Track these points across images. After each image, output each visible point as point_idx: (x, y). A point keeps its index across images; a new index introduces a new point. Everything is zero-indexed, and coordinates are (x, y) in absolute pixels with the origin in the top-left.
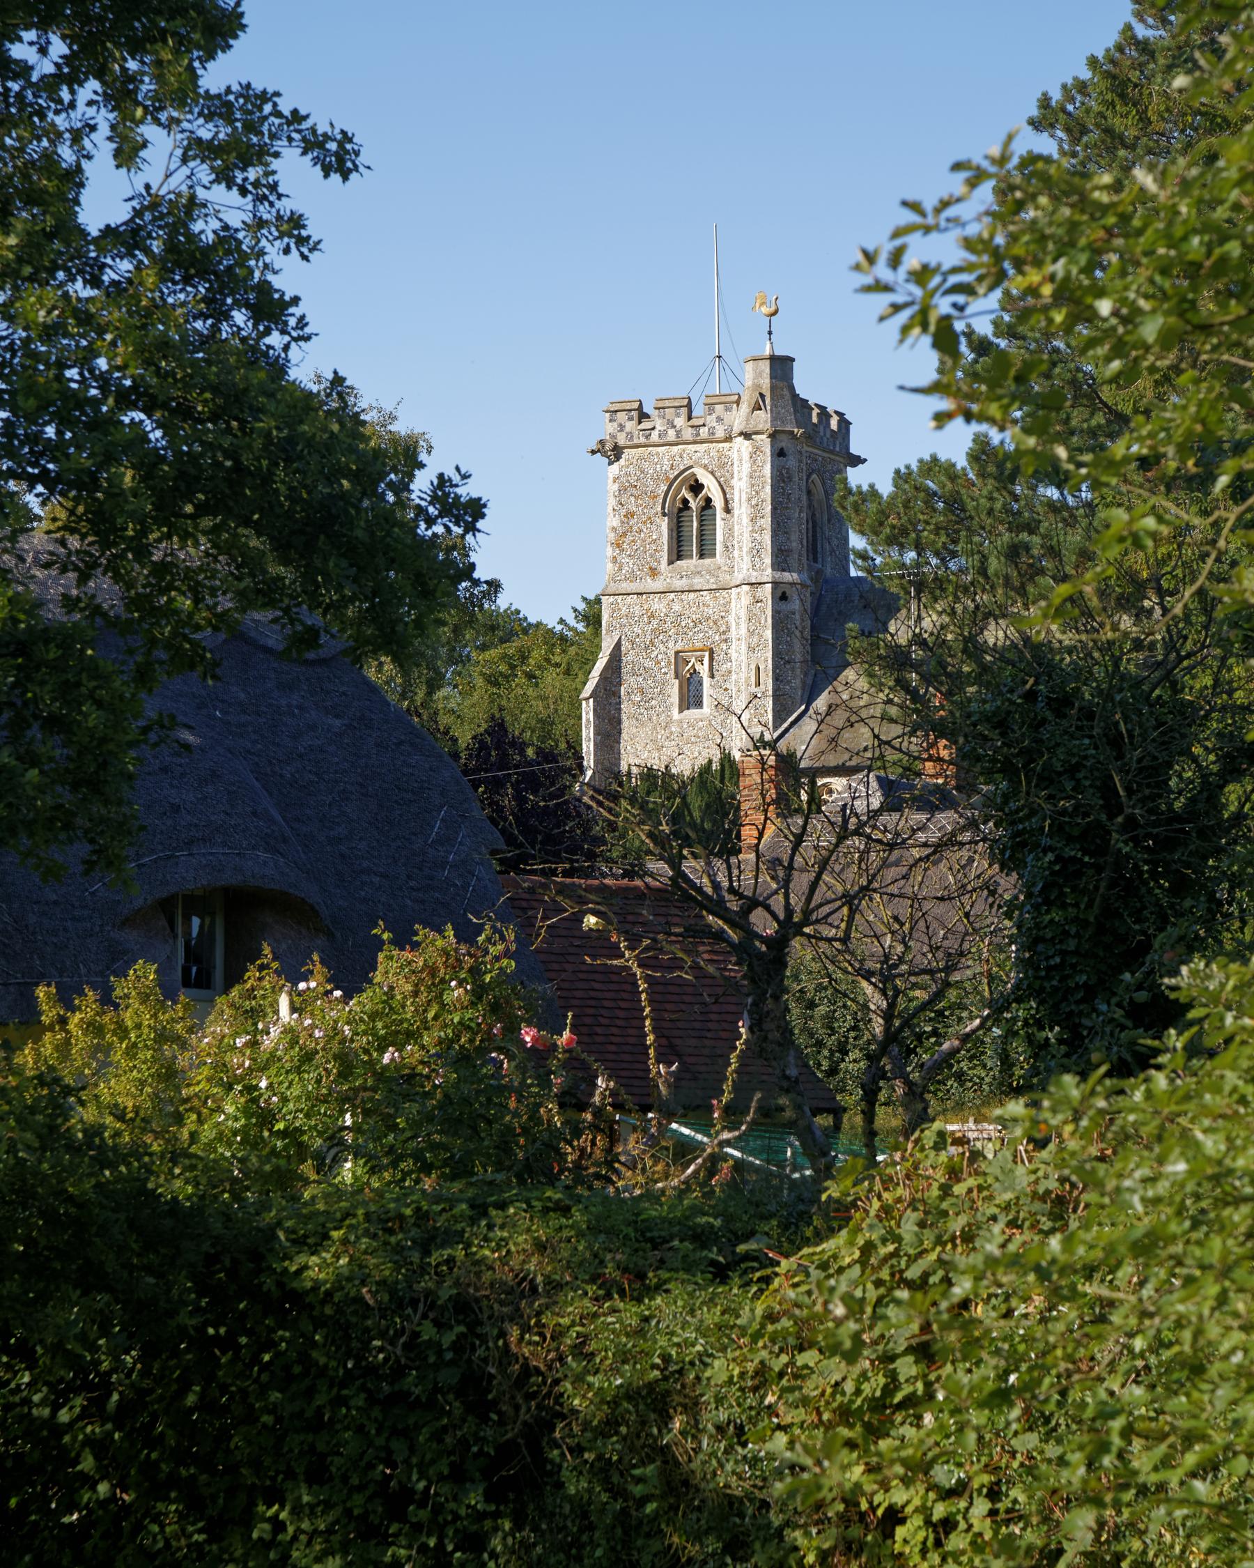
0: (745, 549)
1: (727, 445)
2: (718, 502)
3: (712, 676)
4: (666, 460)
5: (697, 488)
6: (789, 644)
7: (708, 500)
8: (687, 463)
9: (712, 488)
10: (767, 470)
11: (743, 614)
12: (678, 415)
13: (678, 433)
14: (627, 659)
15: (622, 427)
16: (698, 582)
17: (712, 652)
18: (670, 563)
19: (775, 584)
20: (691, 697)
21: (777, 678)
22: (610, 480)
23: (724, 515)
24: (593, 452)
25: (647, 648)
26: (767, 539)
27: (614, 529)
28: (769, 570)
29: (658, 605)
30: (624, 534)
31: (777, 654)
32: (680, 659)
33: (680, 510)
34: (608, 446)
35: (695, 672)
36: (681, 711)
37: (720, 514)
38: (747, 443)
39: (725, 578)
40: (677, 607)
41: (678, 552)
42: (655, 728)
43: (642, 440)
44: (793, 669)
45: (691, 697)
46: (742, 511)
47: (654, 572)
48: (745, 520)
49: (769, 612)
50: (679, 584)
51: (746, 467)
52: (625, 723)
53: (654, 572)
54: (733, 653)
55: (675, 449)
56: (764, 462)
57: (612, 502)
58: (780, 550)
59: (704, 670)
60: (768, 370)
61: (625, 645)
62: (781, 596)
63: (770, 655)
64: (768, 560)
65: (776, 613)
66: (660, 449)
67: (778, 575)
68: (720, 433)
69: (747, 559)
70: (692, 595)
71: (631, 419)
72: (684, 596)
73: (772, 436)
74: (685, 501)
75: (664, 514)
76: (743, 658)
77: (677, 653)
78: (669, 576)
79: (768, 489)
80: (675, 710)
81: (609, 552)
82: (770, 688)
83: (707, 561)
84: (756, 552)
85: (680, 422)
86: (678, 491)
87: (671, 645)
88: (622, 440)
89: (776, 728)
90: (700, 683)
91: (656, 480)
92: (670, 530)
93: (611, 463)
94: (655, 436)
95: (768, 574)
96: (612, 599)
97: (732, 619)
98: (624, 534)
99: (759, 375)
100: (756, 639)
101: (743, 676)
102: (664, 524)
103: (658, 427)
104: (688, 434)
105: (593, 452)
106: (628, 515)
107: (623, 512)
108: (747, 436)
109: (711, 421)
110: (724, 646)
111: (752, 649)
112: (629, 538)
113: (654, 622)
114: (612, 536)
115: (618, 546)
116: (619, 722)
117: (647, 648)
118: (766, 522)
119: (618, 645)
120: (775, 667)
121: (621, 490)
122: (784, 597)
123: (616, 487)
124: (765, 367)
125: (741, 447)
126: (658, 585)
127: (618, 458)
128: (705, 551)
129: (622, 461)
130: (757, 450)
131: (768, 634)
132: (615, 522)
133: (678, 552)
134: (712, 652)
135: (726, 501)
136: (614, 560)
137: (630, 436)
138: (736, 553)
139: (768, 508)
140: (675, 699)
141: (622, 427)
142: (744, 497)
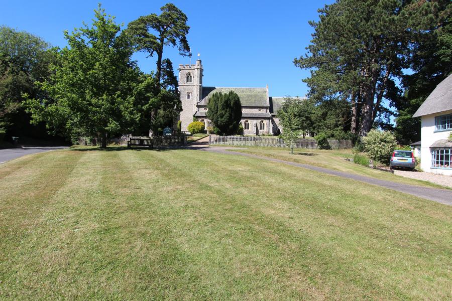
2: (192, 76)
5: (190, 74)
9: (191, 75)
20: (189, 97)
45: (189, 97)
46: (196, 77)
59: (190, 94)
108: (197, 69)
133: (187, 81)
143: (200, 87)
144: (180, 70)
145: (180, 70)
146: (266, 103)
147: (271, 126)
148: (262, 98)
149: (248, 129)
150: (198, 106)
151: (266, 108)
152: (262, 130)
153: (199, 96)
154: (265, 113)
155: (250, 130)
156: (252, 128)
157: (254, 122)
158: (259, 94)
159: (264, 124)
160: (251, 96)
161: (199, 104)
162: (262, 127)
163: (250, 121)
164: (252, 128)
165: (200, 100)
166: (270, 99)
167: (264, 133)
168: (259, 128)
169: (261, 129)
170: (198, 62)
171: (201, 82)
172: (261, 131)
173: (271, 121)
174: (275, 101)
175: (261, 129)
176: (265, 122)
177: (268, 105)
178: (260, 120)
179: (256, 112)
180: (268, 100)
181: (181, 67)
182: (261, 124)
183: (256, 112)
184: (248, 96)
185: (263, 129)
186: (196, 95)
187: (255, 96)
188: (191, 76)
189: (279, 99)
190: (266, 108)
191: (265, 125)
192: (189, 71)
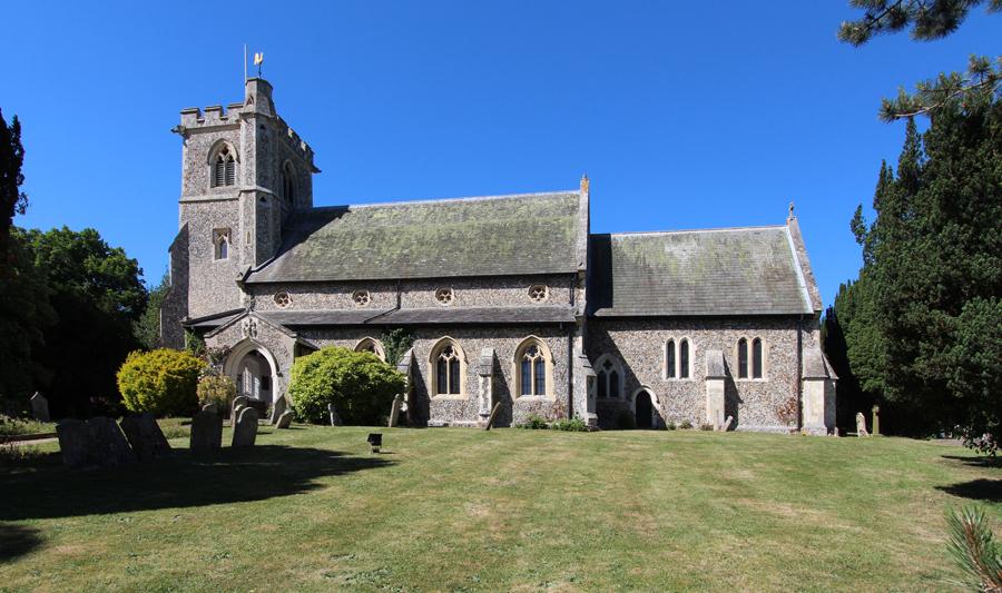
2: (235, 157)
5: (225, 151)
7: (231, 157)
9: (233, 153)
10: (254, 134)
15: (189, 120)
16: (224, 196)
18: (212, 187)
19: (258, 192)
20: (221, 253)
21: (258, 240)
26: (254, 169)
29: (205, 206)
31: (258, 227)
35: (224, 241)
36: (216, 259)
37: (236, 163)
41: (216, 182)
43: (199, 126)
47: (204, 192)
49: (254, 206)
50: (216, 197)
61: (190, 226)
62: (261, 199)
63: (254, 227)
64: (254, 180)
74: (220, 158)
79: (254, 143)
80: (213, 258)
83: (230, 187)
84: (249, 176)
89: (257, 265)
92: (212, 172)
111: (246, 224)
114: (184, 174)
116: (188, 264)
118: (254, 160)
119: (186, 226)
122: (263, 200)
128: (229, 182)
131: (254, 216)
133: (216, 182)
136: (186, 185)
140: (213, 253)
144: (186, 133)
145: (186, 133)
146: (568, 258)
147: (582, 371)
148: (553, 236)
149: (455, 389)
150: (251, 288)
151: (570, 280)
152: (532, 398)
154: (565, 304)
155: (462, 395)
156: (472, 383)
157: (485, 349)
158: (540, 220)
159: (540, 362)
160: (502, 231)
162: (532, 378)
163: (459, 347)
164: (472, 383)
167: (541, 415)
168: (513, 387)
169: (524, 389)
170: (251, 89)
172: (523, 404)
173: (579, 343)
174: (626, 249)
175: (524, 389)
176: (547, 348)
177: (579, 260)
178: (517, 342)
179: (516, 301)
181: (189, 122)
182: (523, 364)
183: (516, 301)
184: (486, 232)
185: (540, 389)
187: (521, 229)
188: (231, 160)
189: (645, 240)
190: (570, 280)
191: (548, 366)
192: (220, 135)
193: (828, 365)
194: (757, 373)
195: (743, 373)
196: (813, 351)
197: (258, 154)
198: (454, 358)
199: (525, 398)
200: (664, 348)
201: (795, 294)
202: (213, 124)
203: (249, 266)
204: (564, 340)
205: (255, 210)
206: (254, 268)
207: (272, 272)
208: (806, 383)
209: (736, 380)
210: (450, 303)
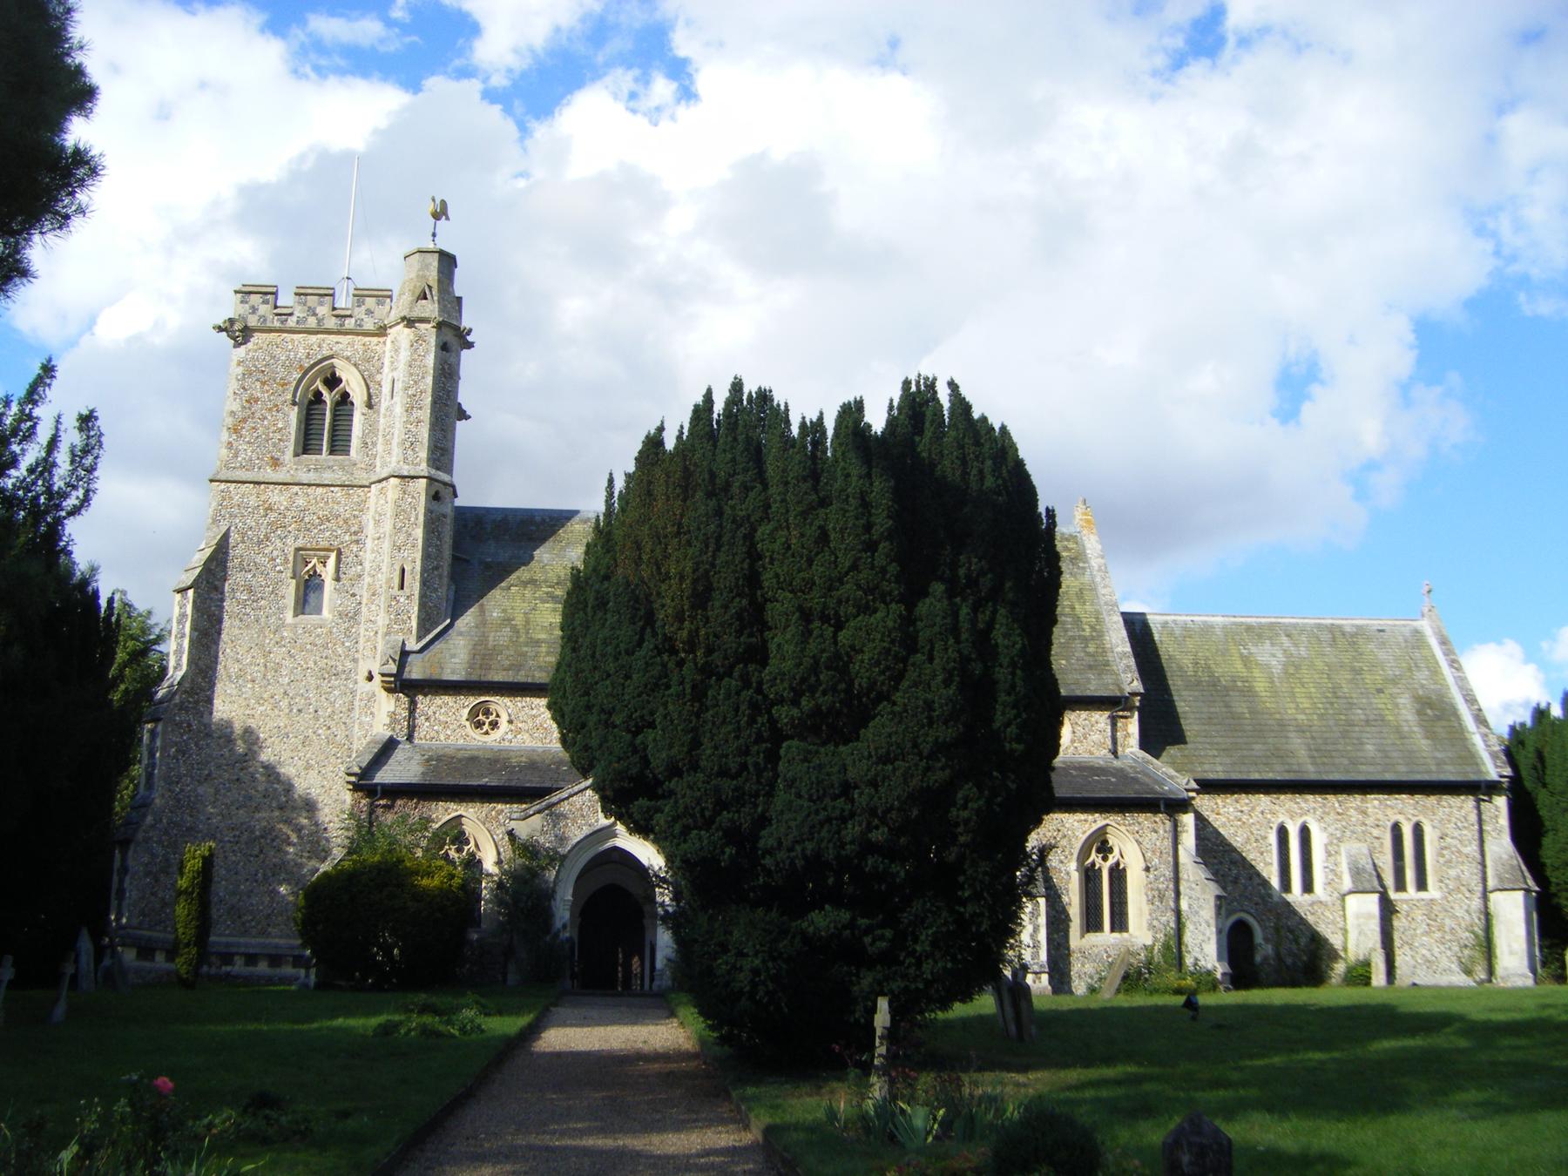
0: (395, 441)
1: (375, 340)
2: (358, 396)
3: (338, 579)
4: (304, 348)
5: (333, 381)
6: (439, 549)
7: (345, 396)
8: (326, 353)
9: (352, 382)
10: (430, 360)
11: (389, 510)
12: (321, 304)
13: (320, 321)
14: (237, 552)
15: (254, 310)
16: (328, 477)
17: (339, 553)
18: (296, 455)
19: (430, 479)
22: (235, 362)
23: (365, 410)
24: (220, 329)
25: (260, 542)
26: (424, 432)
27: (233, 413)
28: (424, 465)
29: (277, 497)
30: (244, 420)
31: (426, 557)
32: (301, 556)
33: (311, 403)
34: (237, 326)
35: (315, 574)
36: (296, 615)
38: (407, 330)
39: (362, 478)
40: (301, 502)
42: (262, 630)
43: (277, 324)
44: (440, 577)
47: (276, 463)
48: (399, 410)
49: (421, 510)
50: (305, 478)
51: (405, 355)
52: (226, 623)
53: (276, 463)
54: (368, 557)
55: (313, 338)
56: (427, 352)
57: (234, 385)
58: (436, 446)
59: (327, 573)
60: (436, 264)
63: (418, 555)
64: (423, 454)
65: (428, 511)
66: (296, 336)
67: (433, 471)
68: (369, 325)
69: (396, 451)
70: (320, 490)
71: (266, 302)
72: (311, 490)
73: (440, 326)
74: (318, 394)
75: (294, 403)
76: (387, 559)
77: (298, 550)
78: (293, 467)
79: (429, 380)
81: (225, 436)
82: (417, 593)
85: (323, 310)
86: (313, 381)
87: (290, 541)
88: (253, 321)
89: (419, 638)
90: (320, 587)
91: (288, 367)
92: (299, 421)
93: (238, 345)
94: (292, 322)
95: (423, 468)
96: (223, 486)
97: (368, 519)
98: (244, 420)
99: (426, 267)
100: (402, 537)
101: (382, 578)
102: (293, 415)
103: (297, 314)
104: (331, 323)
105: (220, 329)
106: (253, 400)
107: (245, 396)
108: (410, 322)
109: (360, 313)
110: (355, 548)
112: (250, 424)
113: (272, 516)
114: (229, 421)
115: (236, 431)
116: (220, 621)
117: (260, 542)
118: (425, 414)
119: (226, 536)
120: (424, 570)
121: (248, 374)
123: (240, 370)
124: (434, 261)
125: (402, 334)
126: (280, 476)
127: (245, 342)
128: (339, 445)
129: (250, 345)
130: (420, 338)
131: (419, 533)
132: (236, 407)
133: (307, 443)
134: (339, 553)
135: (370, 396)
136: (230, 445)
137: (263, 318)
138: (380, 448)
139: (428, 400)
141: (254, 310)
142: (399, 386)
143: (435, 497)
150: (403, 685)
152: (1106, 938)
153: (414, 585)
159: (1118, 874)
161: (415, 671)
165: (425, 625)
166: (1138, 629)
169: (1092, 923)
171: (441, 452)
180: (1118, 641)
185: (1120, 923)
186: (386, 575)
193: (1524, 868)
194: (1422, 885)
195: (1400, 886)
196: (1501, 846)
197: (434, 403)
198: (472, 855)
199: (1093, 938)
200: (1273, 838)
201: (1471, 757)
202: (312, 322)
203: (400, 638)
204: (1161, 821)
205: (421, 518)
206: (413, 645)
207: (454, 658)
208: (1493, 897)
209: (1393, 895)
210: (496, 735)
